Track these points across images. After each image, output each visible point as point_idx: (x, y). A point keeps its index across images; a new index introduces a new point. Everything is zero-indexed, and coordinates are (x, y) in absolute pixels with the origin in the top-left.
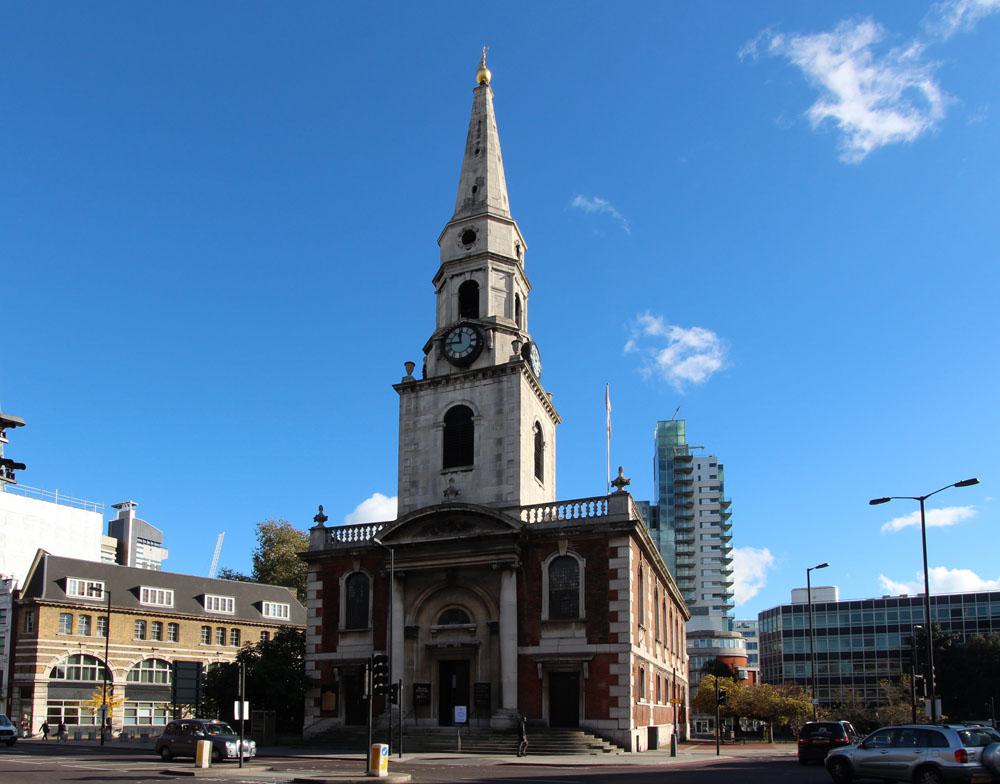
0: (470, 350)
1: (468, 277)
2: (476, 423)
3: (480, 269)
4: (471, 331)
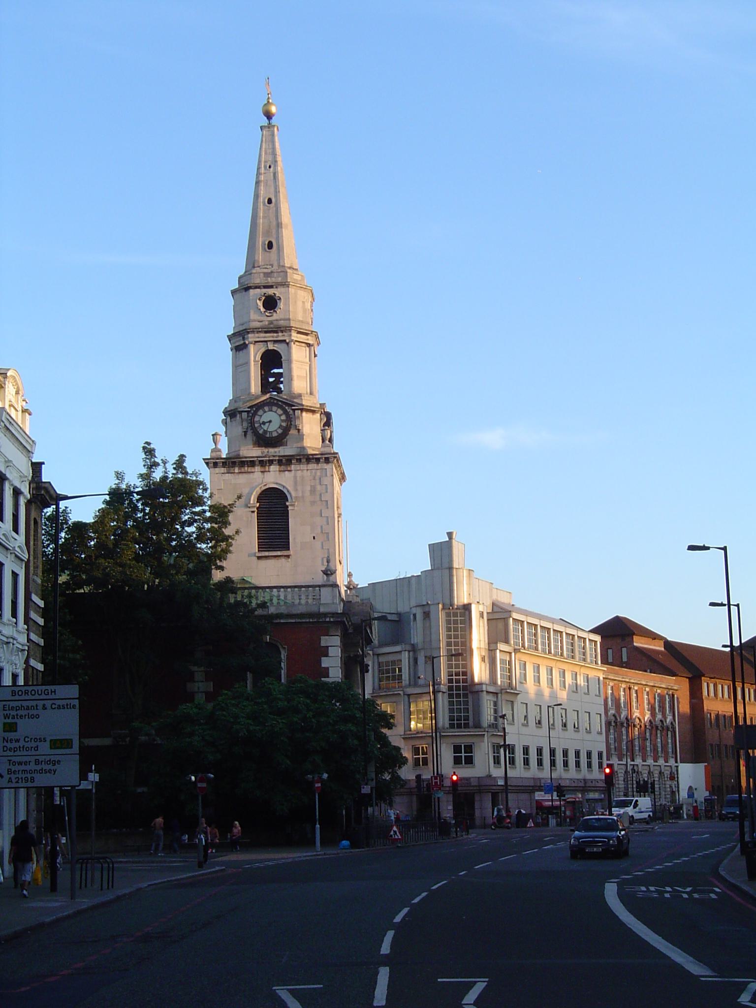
0: (280, 431)
1: (271, 346)
2: (290, 508)
3: (285, 341)
4: (280, 411)
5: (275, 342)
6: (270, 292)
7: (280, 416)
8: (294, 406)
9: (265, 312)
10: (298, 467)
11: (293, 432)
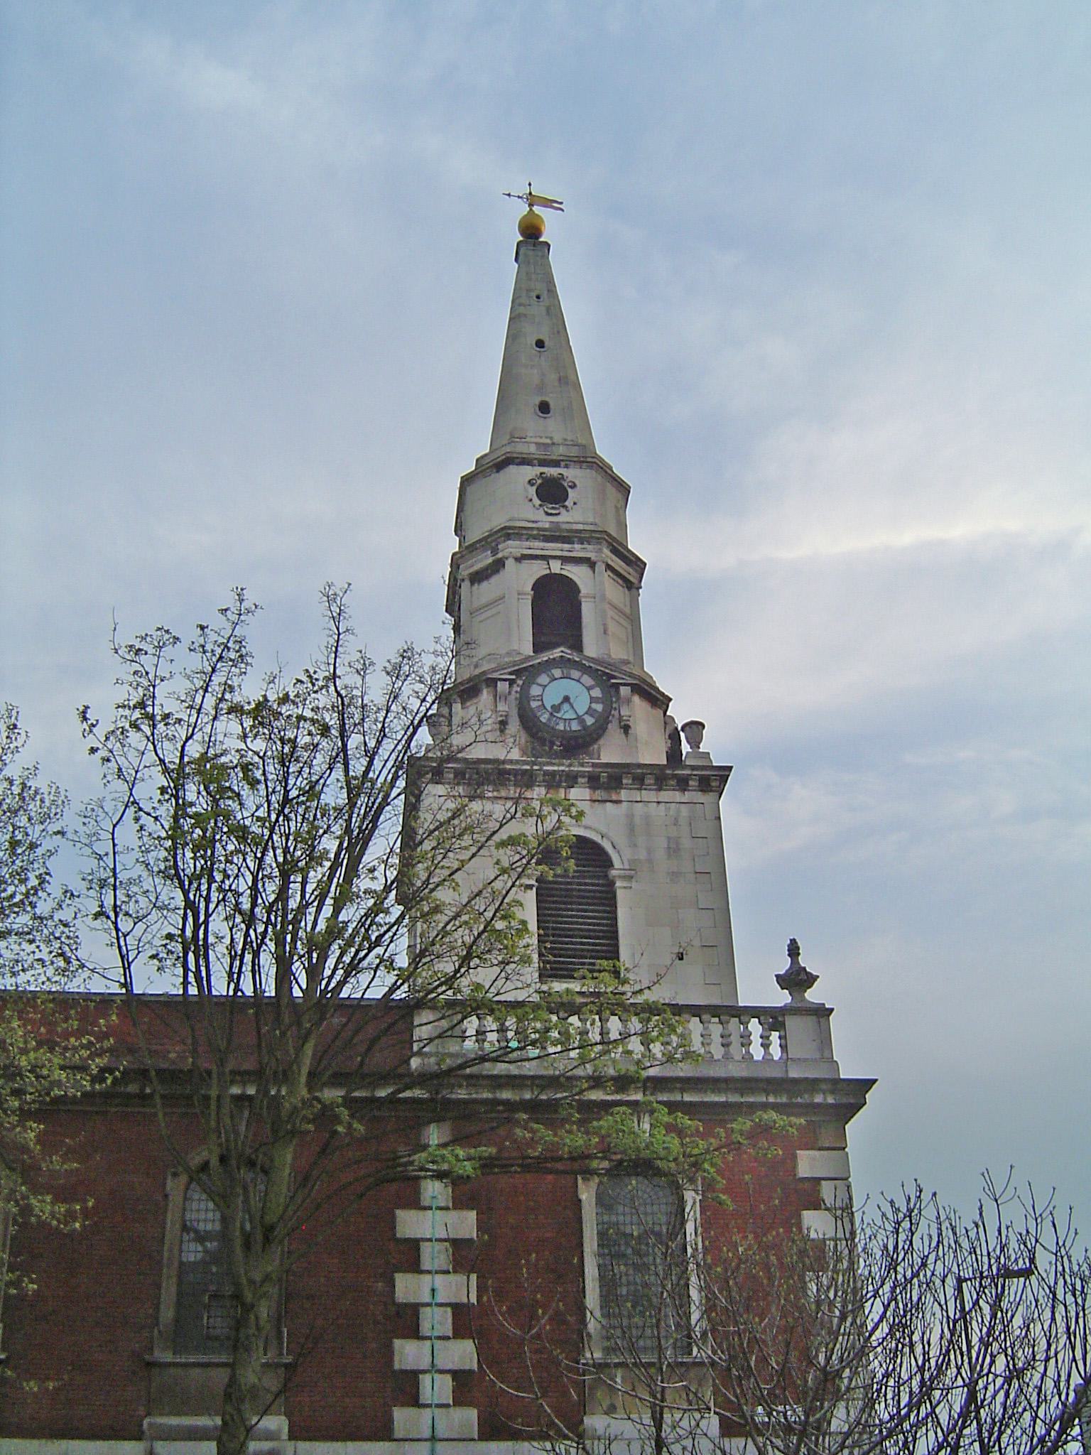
1: (556, 567)
2: (618, 884)
5: (565, 560)
6: (552, 472)
7: (589, 689)
8: (615, 677)
9: (540, 505)
10: (637, 795)
11: (613, 728)
